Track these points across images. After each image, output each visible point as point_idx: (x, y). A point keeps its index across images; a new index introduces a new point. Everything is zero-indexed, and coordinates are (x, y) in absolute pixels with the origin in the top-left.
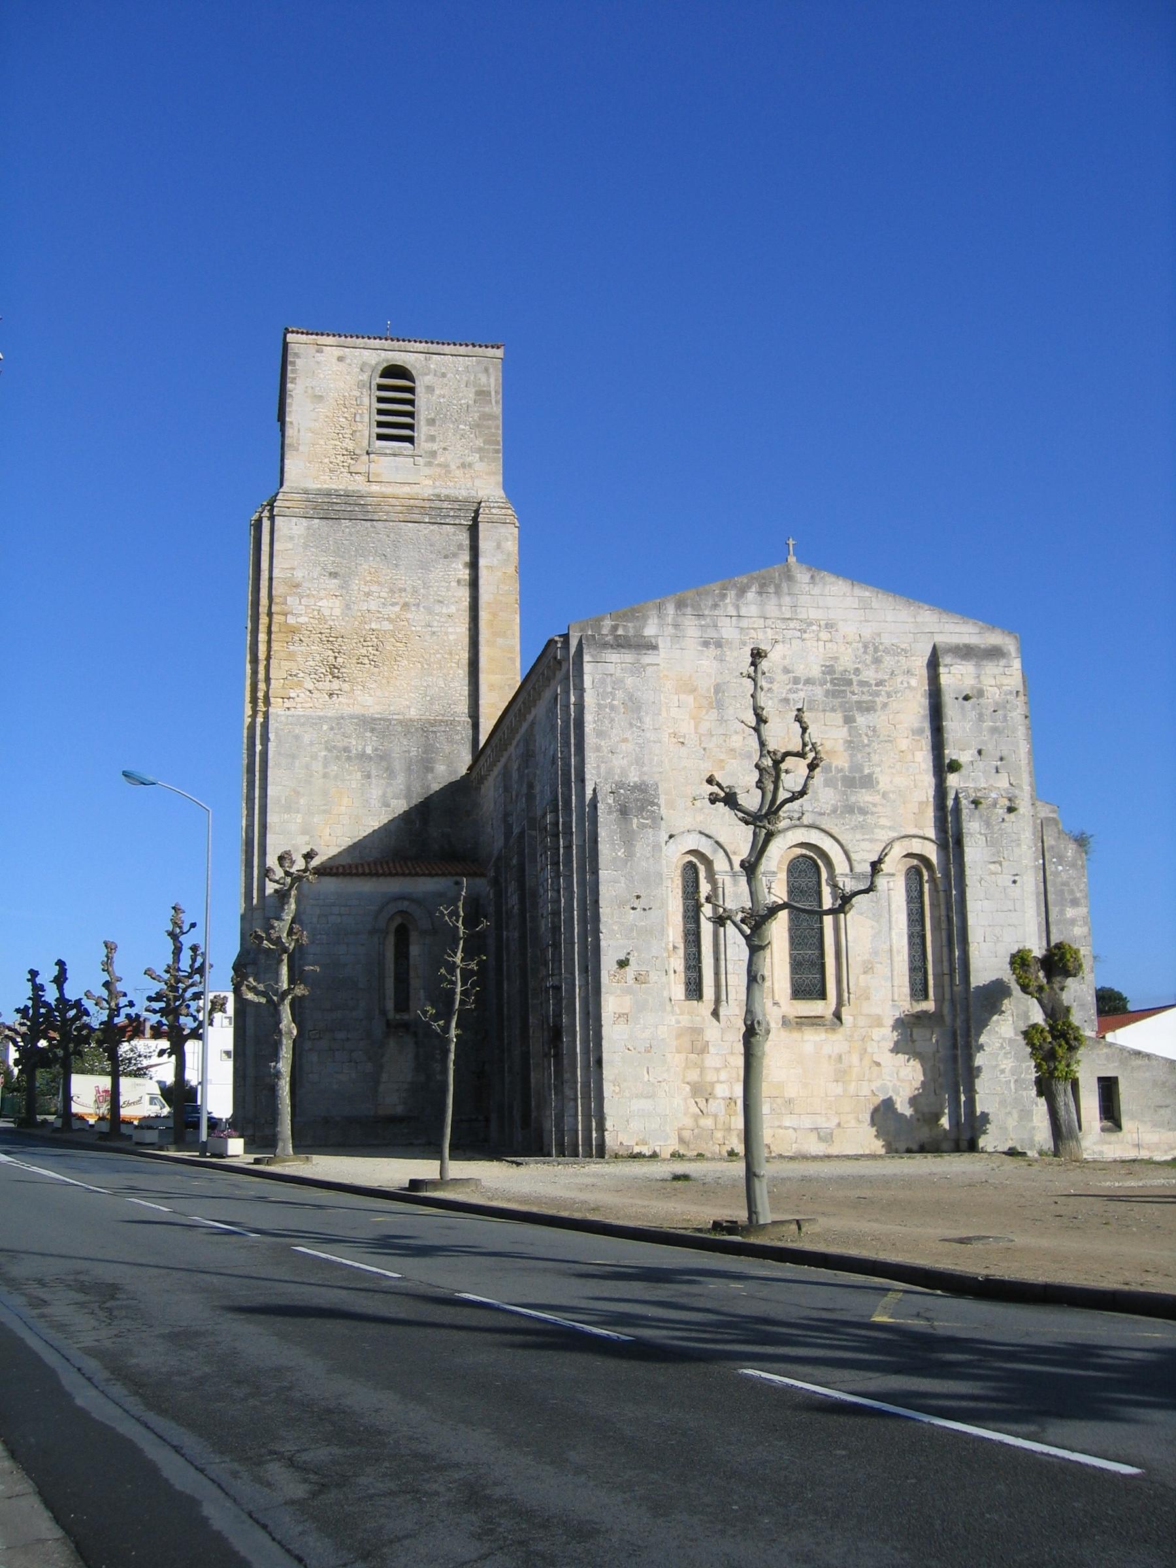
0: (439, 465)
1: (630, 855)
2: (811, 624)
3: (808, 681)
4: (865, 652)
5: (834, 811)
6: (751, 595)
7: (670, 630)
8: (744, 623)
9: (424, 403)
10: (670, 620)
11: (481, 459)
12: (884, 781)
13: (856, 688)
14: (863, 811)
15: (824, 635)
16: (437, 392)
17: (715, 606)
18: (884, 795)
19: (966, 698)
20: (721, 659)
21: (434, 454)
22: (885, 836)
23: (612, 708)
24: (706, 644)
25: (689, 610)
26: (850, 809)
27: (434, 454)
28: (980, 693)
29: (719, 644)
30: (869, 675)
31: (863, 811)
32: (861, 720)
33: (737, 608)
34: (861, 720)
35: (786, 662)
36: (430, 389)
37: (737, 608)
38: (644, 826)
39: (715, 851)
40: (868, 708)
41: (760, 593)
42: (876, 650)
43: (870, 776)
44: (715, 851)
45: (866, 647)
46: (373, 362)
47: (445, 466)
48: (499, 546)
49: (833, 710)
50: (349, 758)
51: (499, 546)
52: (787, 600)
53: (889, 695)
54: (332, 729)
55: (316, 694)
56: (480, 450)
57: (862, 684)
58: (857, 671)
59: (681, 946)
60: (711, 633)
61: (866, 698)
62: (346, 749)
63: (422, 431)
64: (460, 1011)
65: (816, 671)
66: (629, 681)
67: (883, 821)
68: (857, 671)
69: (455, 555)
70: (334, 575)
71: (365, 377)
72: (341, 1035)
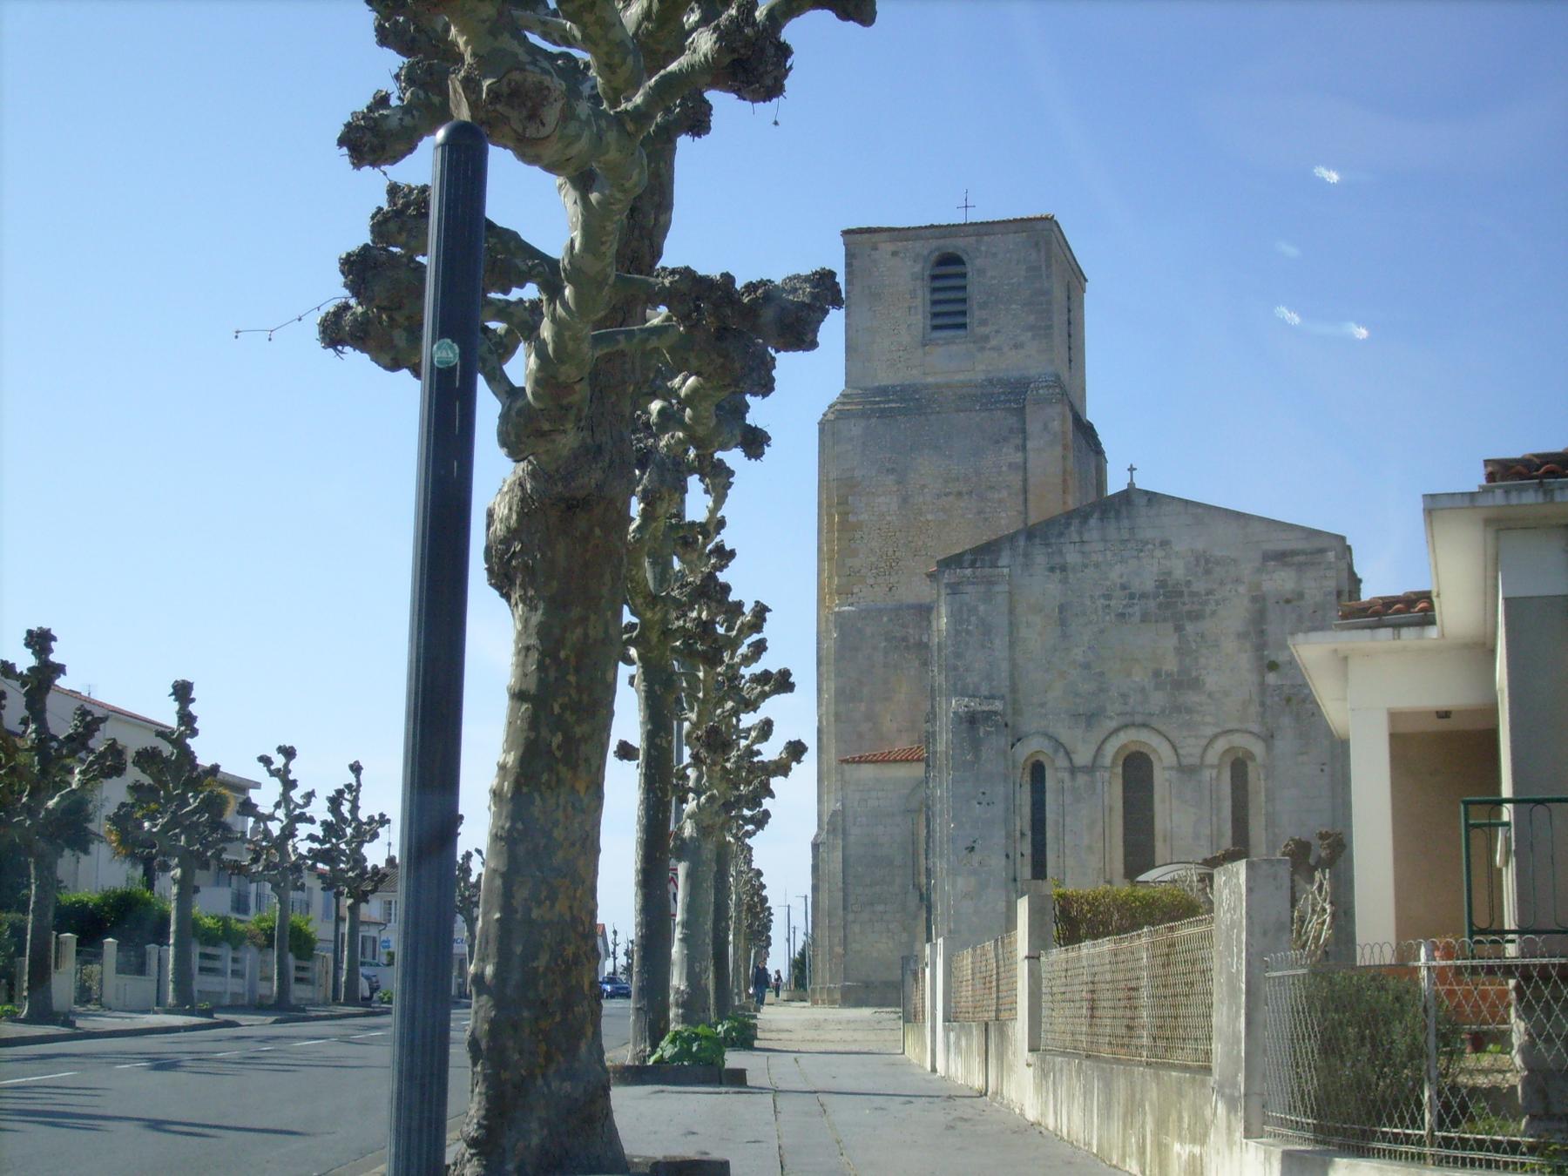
0: (992, 349)
1: (977, 756)
2: (1147, 543)
3: (1143, 596)
4: (1197, 565)
5: (1163, 711)
6: (1093, 522)
7: (1020, 560)
8: (1087, 548)
9: (976, 289)
10: (1021, 550)
11: (1033, 338)
12: (1212, 681)
13: (1186, 599)
14: (1189, 711)
15: (1159, 553)
16: (989, 274)
17: (1061, 534)
18: (1210, 695)
19: (1288, 601)
20: (1064, 581)
21: (986, 338)
22: (1209, 731)
23: (968, 632)
24: (1052, 569)
25: (1037, 541)
26: (1178, 709)
27: (986, 338)
28: (1301, 596)
29: (1063, 569)
30: (1199, 586)
31: (1189, 711)
32: (1189, 628)
33: (1080, 533)
34: (1189, 628)
35: (1124, 579)
36: (981, 272)
37: (1080, 533)
38: (988, 733)
39: (1056, 751)
40: (1196, 616)
41: (1102, 520)
42: (1207, 561)
43: (1197, 679)
44: (1056, 751)
45: (1197, 560)
46: (925, 253)
47: (998, 349)
48: (1046, 427)
49: (1165, 620)
50: (907, 648)
51: (1046, 427)
52: (1126, 523)
53: (1217, 603)
54: (891, 620)
55: (877, 588)
56: (1031, 328)
57: (1193, 594)
58: (1188, 583)
59: (1029, 833)
60: (1057, 560)
61: (1196, 607)
62: (904, 639)
63: (975, 315)
64: (25, 911)
65: (1149, 585)
66: (982, 608)
67: (1208, 719)
68: (1188, 583)
69: (1005, 439)
70: (891, 471)
71: (918, 268)
72: (880, 908)
